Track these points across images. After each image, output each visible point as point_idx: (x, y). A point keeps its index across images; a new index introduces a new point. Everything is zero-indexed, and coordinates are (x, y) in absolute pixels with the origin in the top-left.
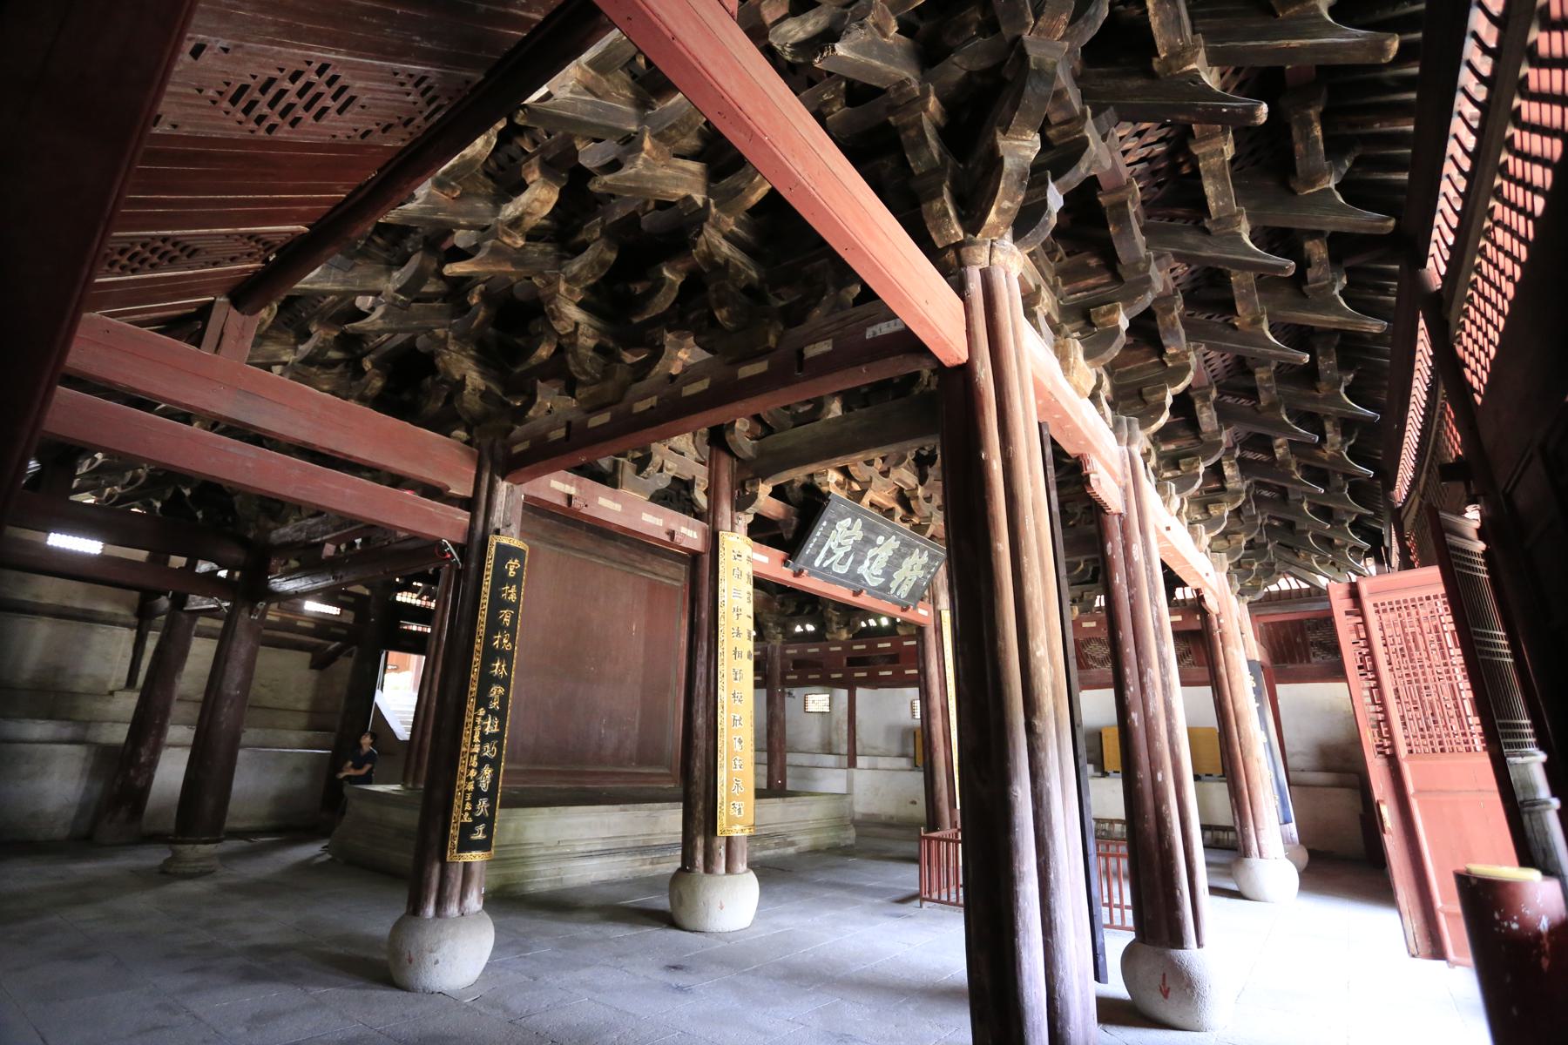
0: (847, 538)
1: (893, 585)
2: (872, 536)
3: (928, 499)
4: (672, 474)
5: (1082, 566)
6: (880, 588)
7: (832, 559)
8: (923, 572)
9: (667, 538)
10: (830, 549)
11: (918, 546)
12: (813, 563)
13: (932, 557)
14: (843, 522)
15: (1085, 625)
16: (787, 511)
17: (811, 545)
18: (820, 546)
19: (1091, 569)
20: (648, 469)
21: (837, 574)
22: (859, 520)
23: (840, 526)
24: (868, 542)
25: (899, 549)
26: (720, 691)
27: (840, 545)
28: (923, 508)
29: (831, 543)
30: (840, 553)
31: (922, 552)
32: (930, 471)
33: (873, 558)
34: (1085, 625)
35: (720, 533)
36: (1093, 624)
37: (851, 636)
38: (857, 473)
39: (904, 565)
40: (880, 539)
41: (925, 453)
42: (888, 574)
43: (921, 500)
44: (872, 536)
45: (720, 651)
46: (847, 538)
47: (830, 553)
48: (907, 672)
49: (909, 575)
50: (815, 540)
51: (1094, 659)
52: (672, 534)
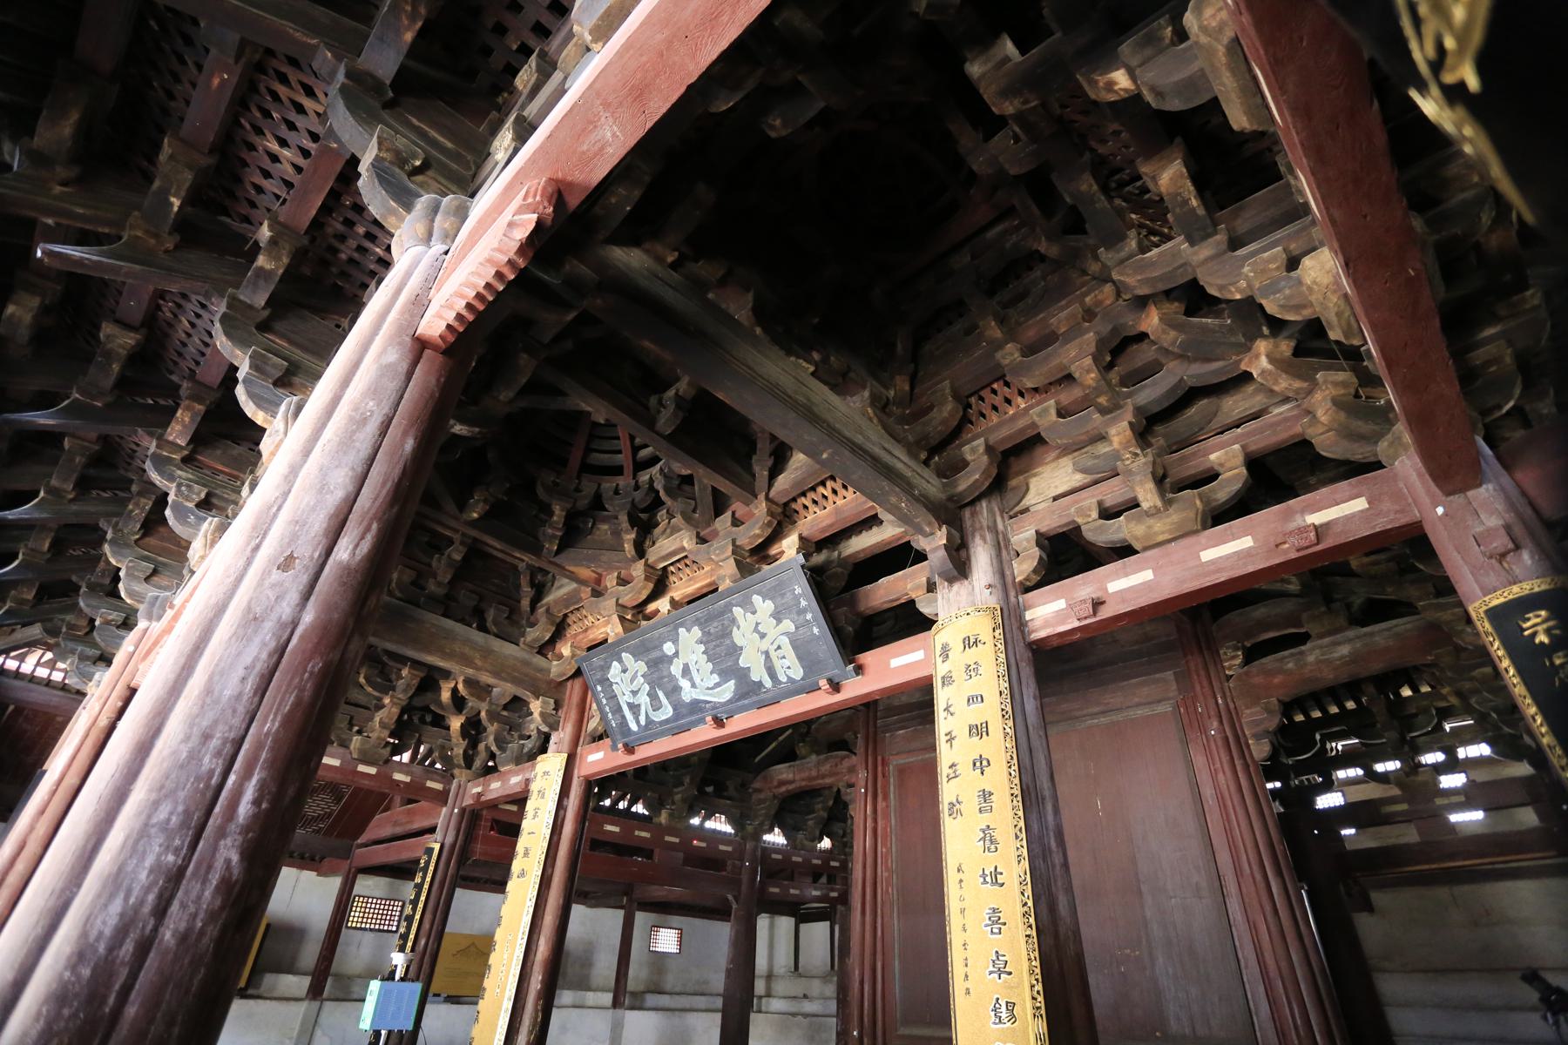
1: (758, 674)
2: (655, 654)
6: (740, 695)
10: (632, 706)
12: (629, 729)
14: (612, 671)
17: (610, 715)
21: (667, 721)
22: (623, 654)
23: (616, 676)
24: (658, 664)
25: (706, 634)
27: (634, 693)
29: (624, 700)
30: (643, 700)
33: (686, 671)
40: (668, 648)
44: (655, 654)
46: (632, 681)
47: (634, 708)
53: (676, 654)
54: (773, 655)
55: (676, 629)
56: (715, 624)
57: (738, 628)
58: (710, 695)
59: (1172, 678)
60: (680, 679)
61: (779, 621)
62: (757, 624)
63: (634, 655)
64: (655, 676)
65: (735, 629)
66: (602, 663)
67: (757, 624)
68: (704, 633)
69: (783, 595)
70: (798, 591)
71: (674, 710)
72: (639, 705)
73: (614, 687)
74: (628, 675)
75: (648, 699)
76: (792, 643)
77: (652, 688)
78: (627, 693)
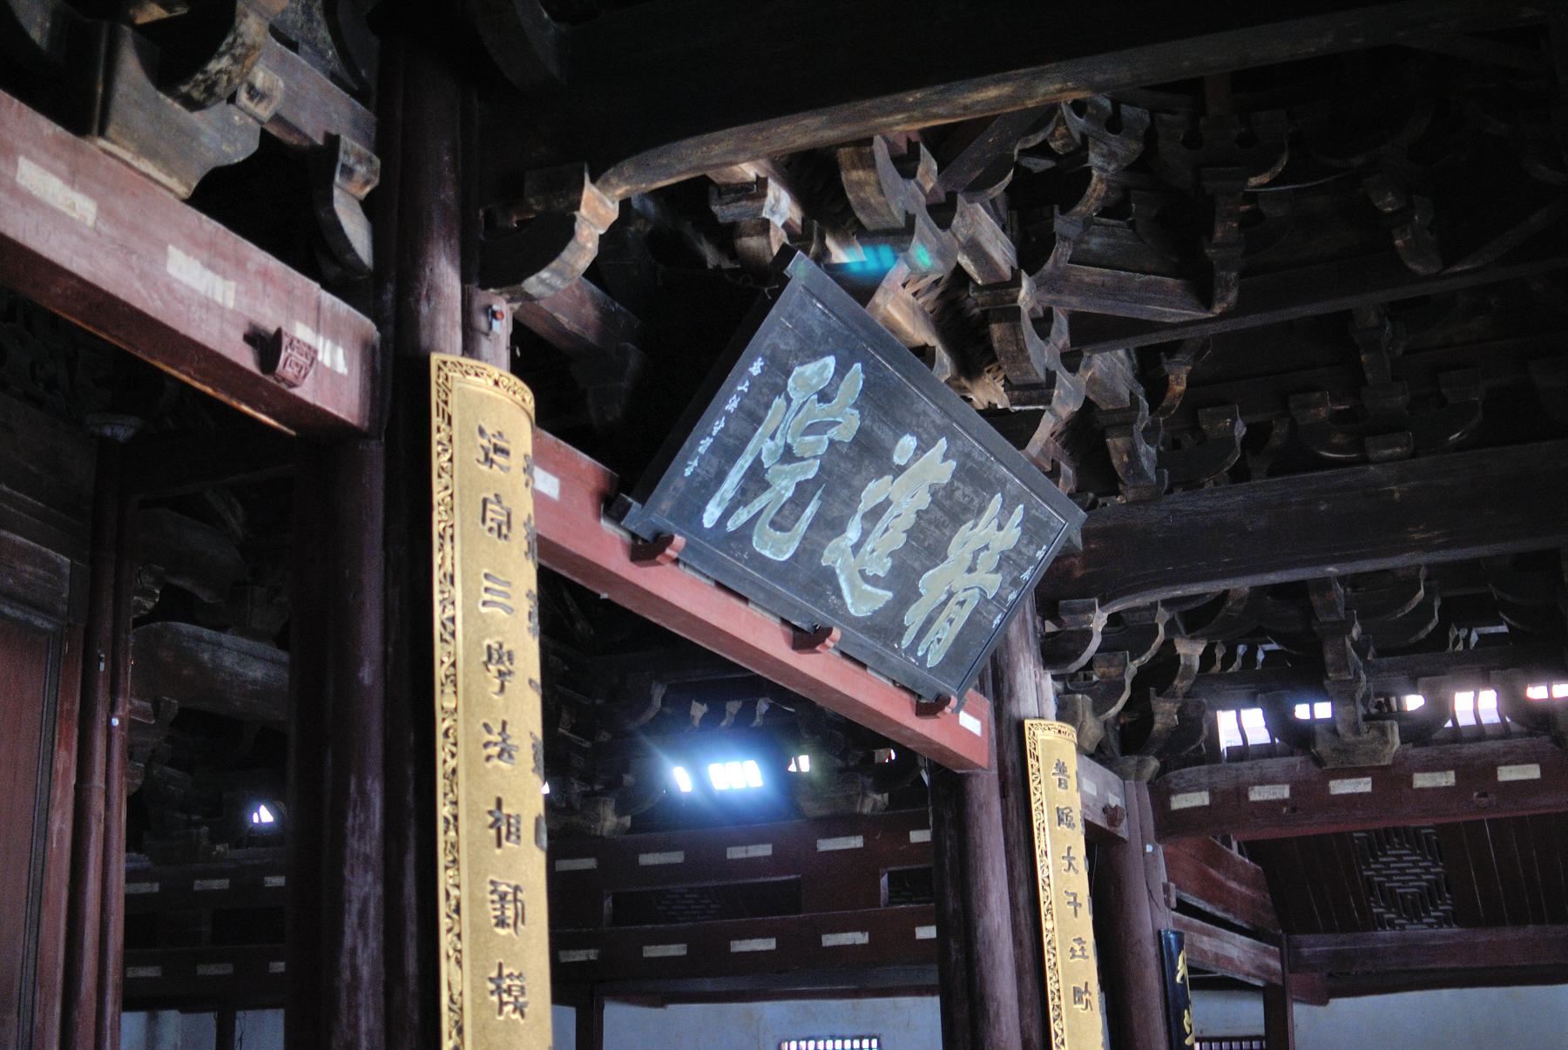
0: (813, 429)
1: (914, 617)
2: (883, 433)
3: (1043, 324)
4: (264, 111)
5: (1422, 592)
7: (756, 506)
8: (998, 577)
9: (247, 359)
11: (1002, 483)
12: (701, 510)
13: (1033, 529)
14: (810, 369)
15: (1422, 780)
16: (606, 317)
17: (706, 443)
18: (729, 451)
19: (1437, 604)
20: (213, 66)
22: (858, 366)
25: (949, 489)
26: (447, 969)
27: (788, 455)
28: (1031, 351)
29: (763, 445)
30: (784, 486)
31: (1007, 509)
32: (1060, 224)
33: (876, 513)
34: (1422, 780)
35: (435, 359)
36: (1447, 779)
37: (627, 821)
38: (870, 194)
39: (954, 550)
41: (1041, 165)
42: (903, 581)
43: (1027, 326)
45: (444, 811)
46: (813, 429)
47: (756, 480)
48: (829, 940)
49: (961, 581)
50: (718, 426)
51: (1391, 899)
52: (267, 345)
53: (901, 470)
54: (953, 601)
55: (942, 431)
56: (968, 490)
57: (975, 526)
58: (853, 587)
59: (67, 571)
60: (858, 517)
61: (998, 569)
62: (986, 547)
63: (868, 386)
64: (845, 466)
65: (970, 524)
66: (818, 331)
67: (986, 547)
68: (951, 483)
69: (1030, 542)
70: (1040, 554)
71: (795, 556)
72: (766, 486)
73: (779, 402)
74: (821, 412)
75: (789, 494)
76: (976, 611)
77: (816, 481)
78: (779, 441)
